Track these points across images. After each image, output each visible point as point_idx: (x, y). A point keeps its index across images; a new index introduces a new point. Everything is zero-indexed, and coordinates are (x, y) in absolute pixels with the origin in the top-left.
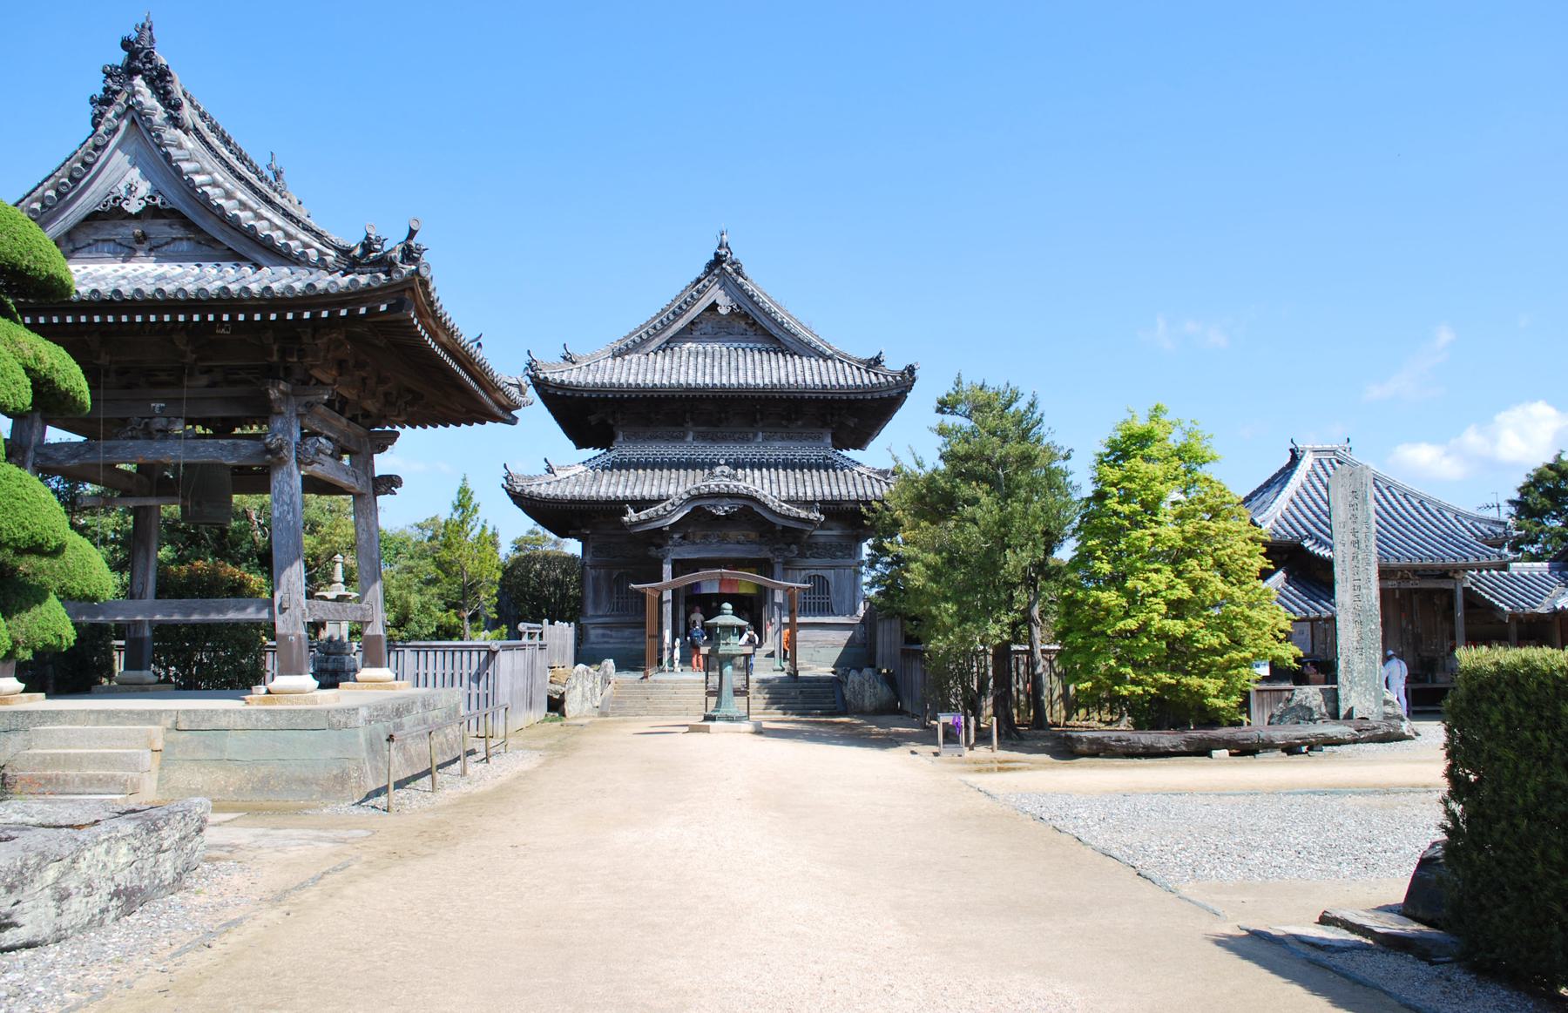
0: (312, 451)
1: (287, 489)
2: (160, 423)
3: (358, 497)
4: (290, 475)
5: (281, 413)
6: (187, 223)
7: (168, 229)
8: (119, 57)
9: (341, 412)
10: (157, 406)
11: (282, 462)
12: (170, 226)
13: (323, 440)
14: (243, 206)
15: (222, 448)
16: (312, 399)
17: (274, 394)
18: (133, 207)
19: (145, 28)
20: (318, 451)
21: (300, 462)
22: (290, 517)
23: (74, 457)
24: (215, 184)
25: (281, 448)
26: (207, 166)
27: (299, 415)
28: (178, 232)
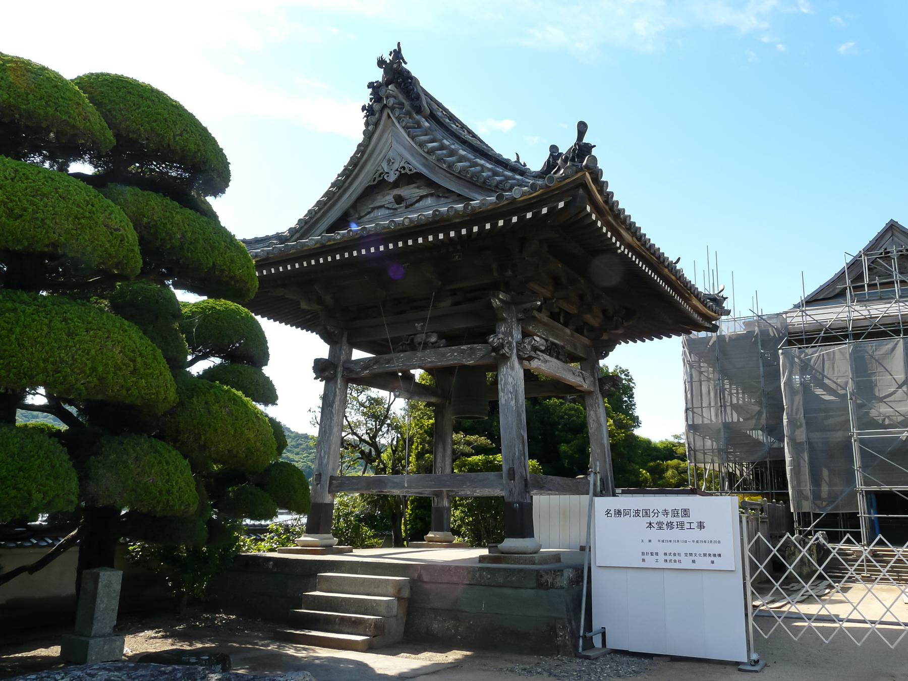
0: (528, 348)
1: (510, 380)
2: (420, 338)
4: (512, 368)
5: (504, 320)
6: (430, 183)
7: (417, 190)
8: (378, 75)
9: (566, 325)
10: (418, 326)
11: (505, 358)
12: (418, 187)
13: (537, 339)
14: (462, 159)
15: (463, 352)
16: (528, 305)
17: (496, 303)
18: (392, 178)
19: (397, 54)
20: (535, 349)
21: (521, 359)
22: (513, 403)
23: (366, 368)
24: (442, 147)
25: (502, 346)
26: (439, 137)
27: (519, 320)
28: (423, 192)
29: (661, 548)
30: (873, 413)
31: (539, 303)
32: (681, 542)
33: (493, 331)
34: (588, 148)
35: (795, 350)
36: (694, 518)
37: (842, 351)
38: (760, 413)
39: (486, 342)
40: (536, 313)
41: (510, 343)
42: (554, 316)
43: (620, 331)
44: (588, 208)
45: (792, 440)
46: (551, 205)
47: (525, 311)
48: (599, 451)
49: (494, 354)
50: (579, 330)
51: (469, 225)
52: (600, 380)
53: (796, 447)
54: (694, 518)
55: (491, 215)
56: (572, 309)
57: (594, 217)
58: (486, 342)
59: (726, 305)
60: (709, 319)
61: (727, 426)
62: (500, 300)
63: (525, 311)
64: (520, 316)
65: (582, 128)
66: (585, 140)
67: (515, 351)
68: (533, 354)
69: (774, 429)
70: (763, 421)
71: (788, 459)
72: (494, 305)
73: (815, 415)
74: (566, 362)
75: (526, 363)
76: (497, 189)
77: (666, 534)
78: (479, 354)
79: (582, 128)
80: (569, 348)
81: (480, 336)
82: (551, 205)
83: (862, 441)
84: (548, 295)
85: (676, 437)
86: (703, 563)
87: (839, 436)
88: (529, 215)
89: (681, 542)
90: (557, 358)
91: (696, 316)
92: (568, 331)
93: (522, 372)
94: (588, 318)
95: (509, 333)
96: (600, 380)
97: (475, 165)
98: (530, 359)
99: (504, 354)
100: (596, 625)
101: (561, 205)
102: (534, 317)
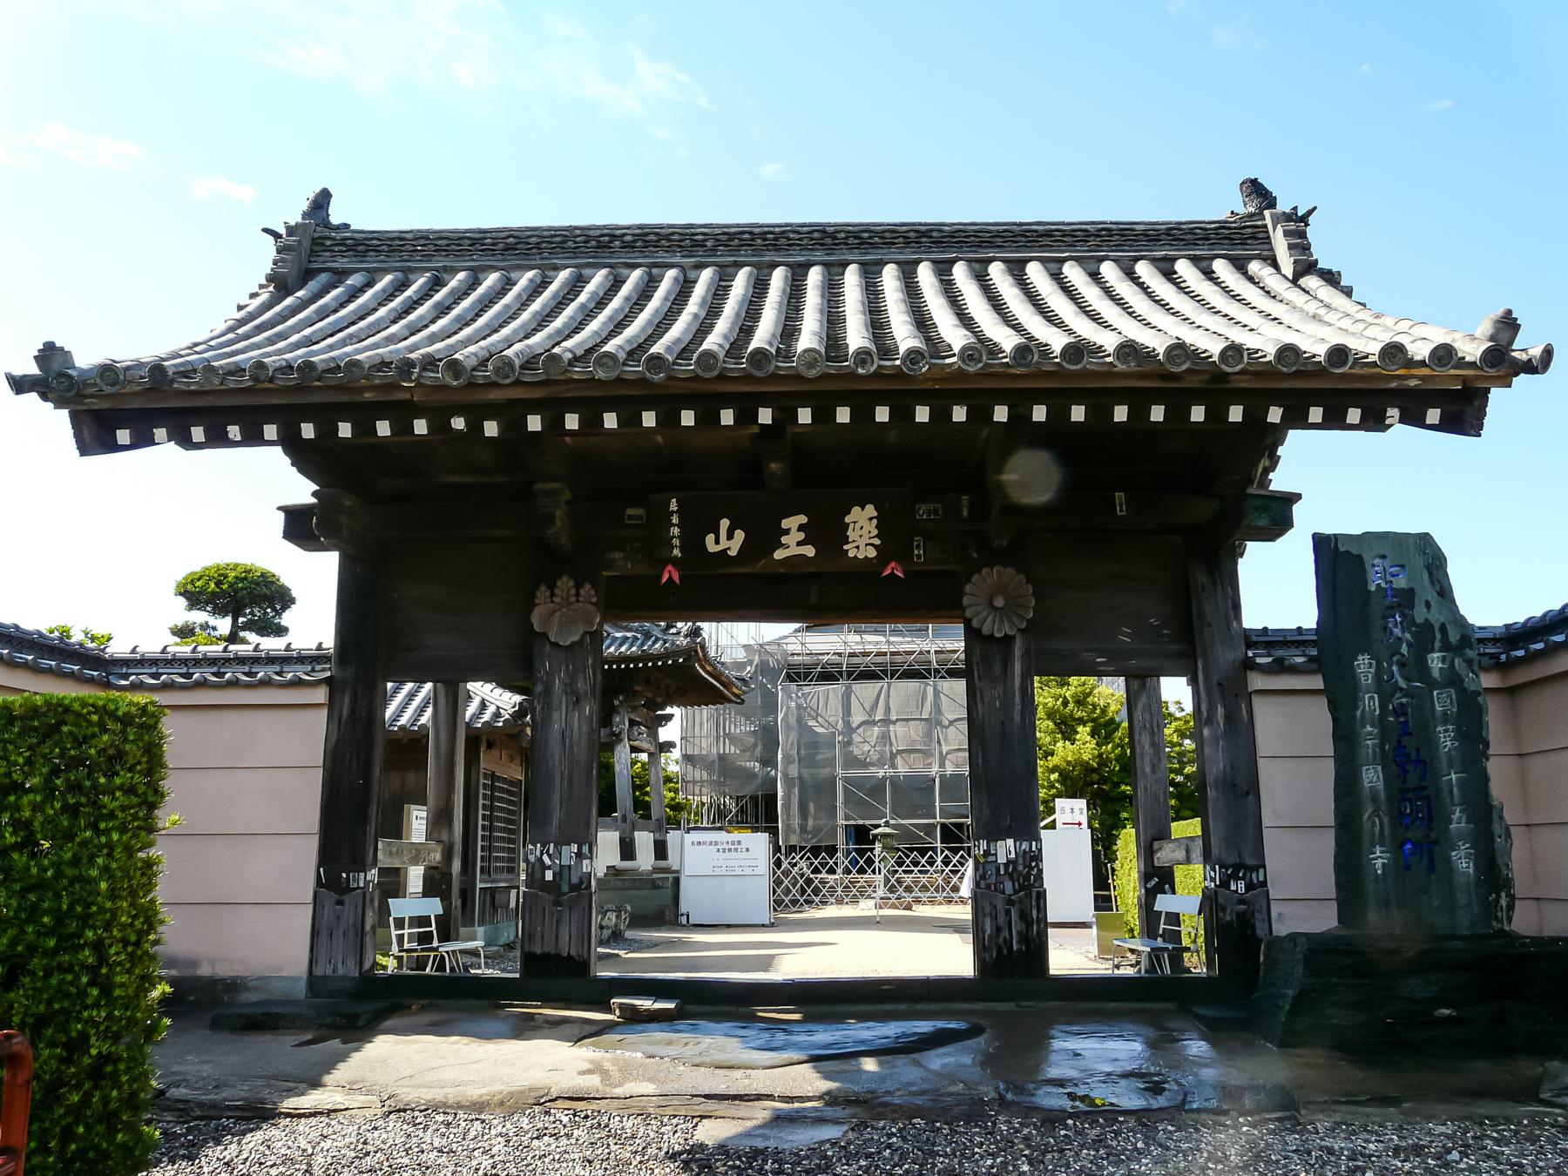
3: (651, 755)
29: (724, 863)
30: (856, 751)
32: (736, 860)
35: (793, 686)
36: (744, 846)
37: (835, 690)
38: (755, 745)
45: (785, 775)
53: (788, 781)
54: (744, 846)
55: (634, 659)
61: (722, 758)
69: (768, 761)
70: (758, 752)
71: (780, 794)
73: (811, 747)
77: (728, 854)
83: (846, 780)
84: (650, 695)
86: (748, 871)
87: (826, 772)
89: (736, 860)
100: (683, 910)
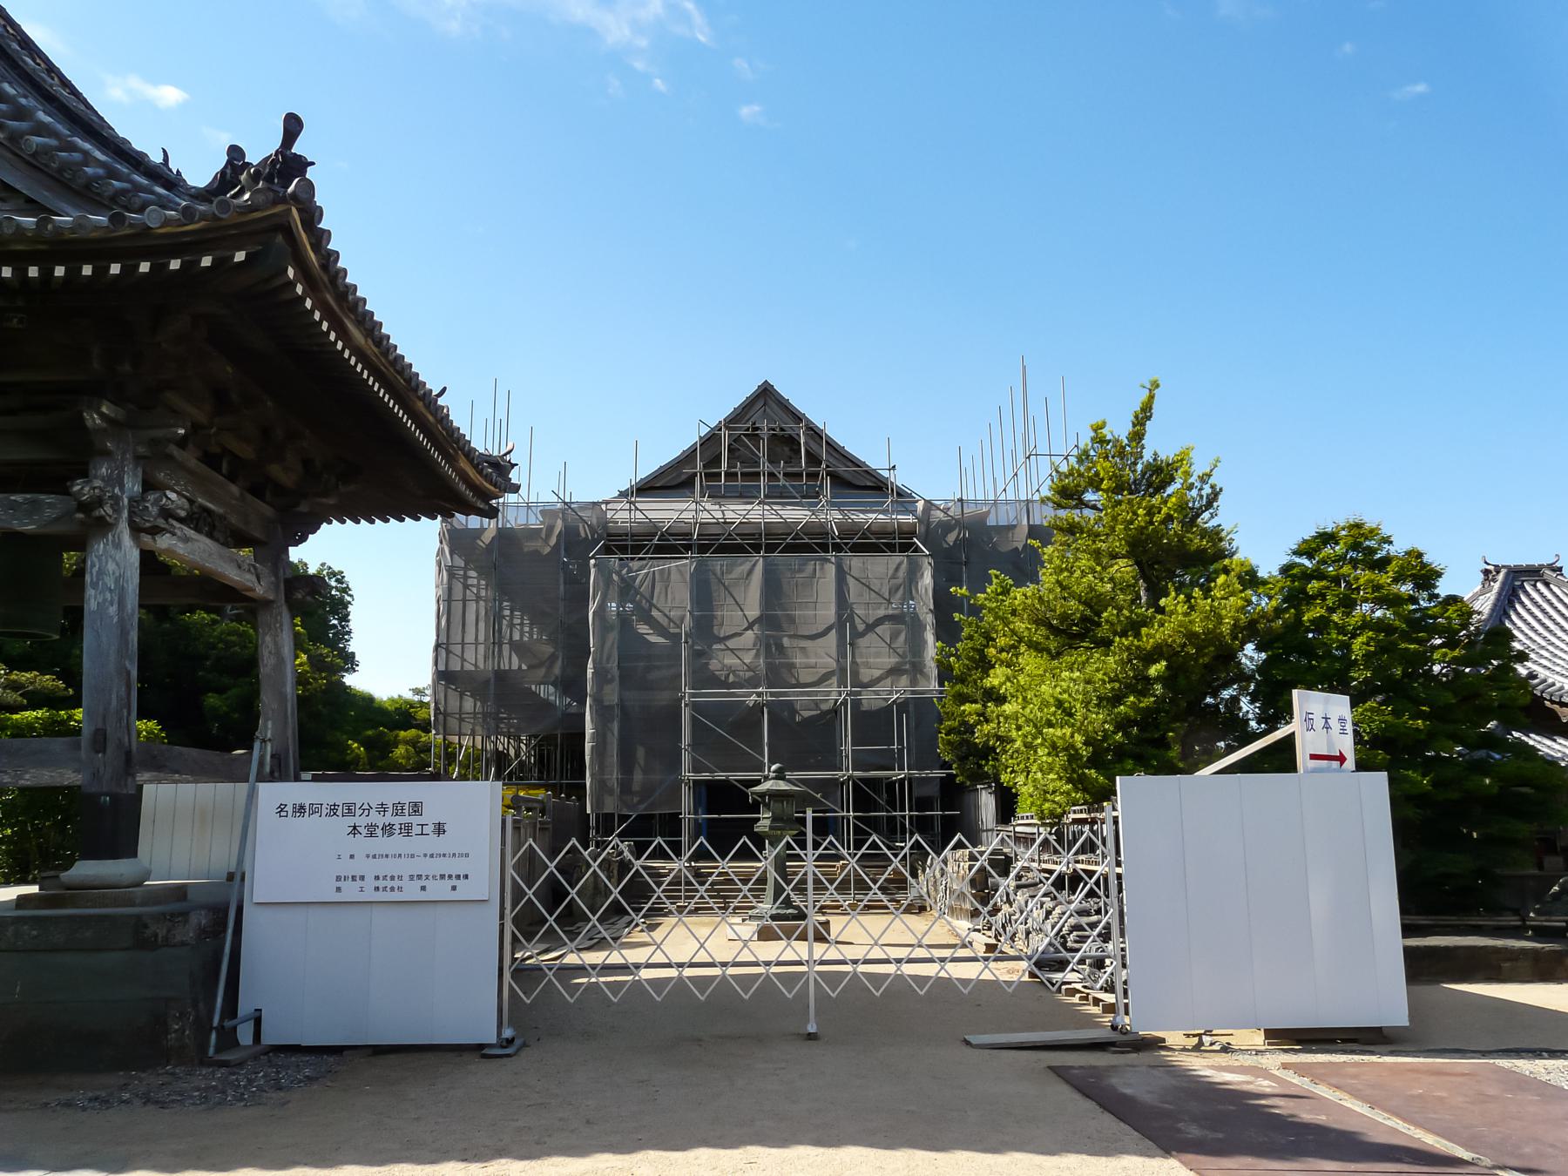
0: (154, 510)
1: (111, 566)
4: (118, 545)
5: (107, 454)
9: (232, 478)
11: (104, 526)
13: (173, 496)
14: (41, 129)
15: (14, 506)
16: (159, 433)
17: (93, 420)
20: (167, 514)
21: (136, 530)
22: (113, 610)
25: (99, 502)
27: (138, 458)
29: (370, 868)
30: (714, 665)
31: (182, 431)
32: (405, 859)
33: (84, 474)
34: (301, 165)
35: (614, 561)
36: (429, 817)
37: (683, 566)
38: (553, 658)
39: (66, 492)
40: (174, 450)
41: (116, 500)
42: (211, 460)
43: (331, 501)
44: (291, 272)
45: (597, 701)
46: (219, 253)
47: (154, 443)
48: (275, 706)
49: (80, 516)
50: (256, 491)
51: (46, 260)
52: (287, 581)
53: (602, 712)
54: (429, 817)
55: (100, 251)
56: (247, 452)
57: (299, 289)
58: (66, 492)
59: (514, 476)
60: (486, 496)
61: (501, 676)
62: (102, 415)
63: (154, 443)
64: (141, 450)
65: (293, 126)
66: (297, 149)
67: (125, 514)
68: (161, 522)
69: (572, 685)
70: (557, 670)
71: (589, 730)
72: (89, 423)
73: (636, 665)
74: (226, 544)
75: (146, 538)
76: (115, 203)
77: (381, 843)
78: (49, 513)
79: (293, 126)
80: (234, 520)
81: (54, 479)
82: (219, 253)
83: (695, 707)
84: (202, 418)
85: (417, 691)
86: (438, 890)
87: (662, 698)
88: (175, 265)
89: (405, 859)
90: (210, 535)
91: (462, 487)
92: (234, 489)
93: (134, 556)
94: (275, 470)
95: (117, 480)
96: (287, 581)
97: (73, 148)
98: (155, 531)
99: (101, 518)
100: (245, 1007)
101: (240, 256)
102: (170, 457)
